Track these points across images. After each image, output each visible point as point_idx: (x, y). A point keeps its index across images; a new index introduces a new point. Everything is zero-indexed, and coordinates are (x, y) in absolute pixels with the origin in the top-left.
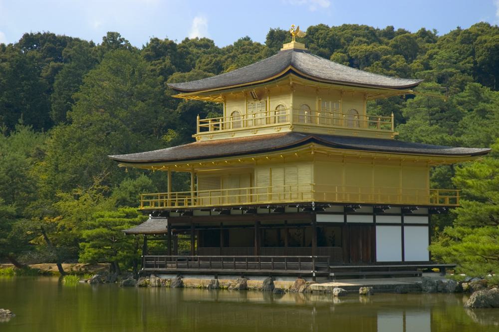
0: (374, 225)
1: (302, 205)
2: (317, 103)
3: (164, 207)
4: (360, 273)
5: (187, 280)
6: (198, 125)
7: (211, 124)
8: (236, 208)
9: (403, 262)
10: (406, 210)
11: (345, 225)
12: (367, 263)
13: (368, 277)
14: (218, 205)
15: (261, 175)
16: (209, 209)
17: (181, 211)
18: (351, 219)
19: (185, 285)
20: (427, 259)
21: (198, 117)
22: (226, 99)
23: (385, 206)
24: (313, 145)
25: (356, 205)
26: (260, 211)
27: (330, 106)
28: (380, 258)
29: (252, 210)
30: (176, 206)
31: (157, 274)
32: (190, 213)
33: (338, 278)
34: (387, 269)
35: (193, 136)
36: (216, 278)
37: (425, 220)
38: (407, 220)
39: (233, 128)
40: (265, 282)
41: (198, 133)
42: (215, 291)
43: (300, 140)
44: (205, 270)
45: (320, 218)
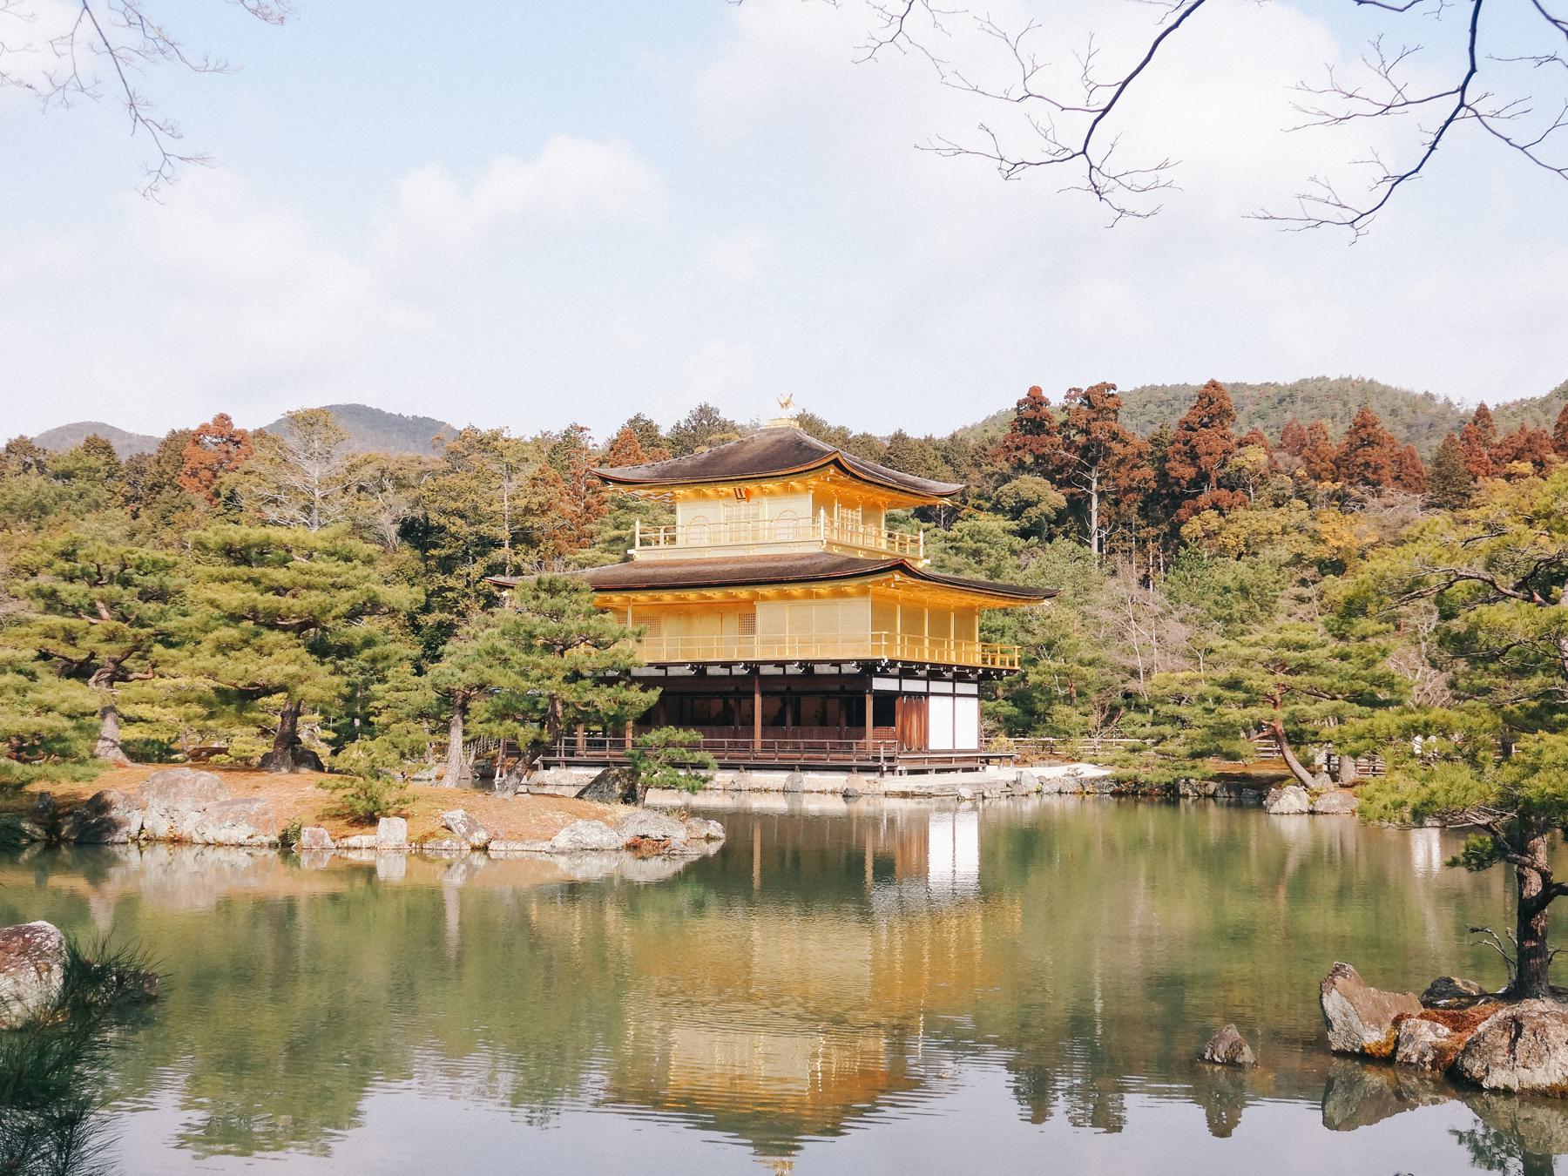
0: (927, 695)
1: (860, 663)
10: (961, 676)
11: (899, 694)
18: (910, 686)
20: (975, 747)
23: (949, 667)
24: (897, 577)
25: (922, 665)
26: (766, 670)
27: (848, 513)
29: (753, 667)
31: (569, 764)
33: (911, 772)
37: (973, 689)
38: (961, 688)
45: (879, 684)
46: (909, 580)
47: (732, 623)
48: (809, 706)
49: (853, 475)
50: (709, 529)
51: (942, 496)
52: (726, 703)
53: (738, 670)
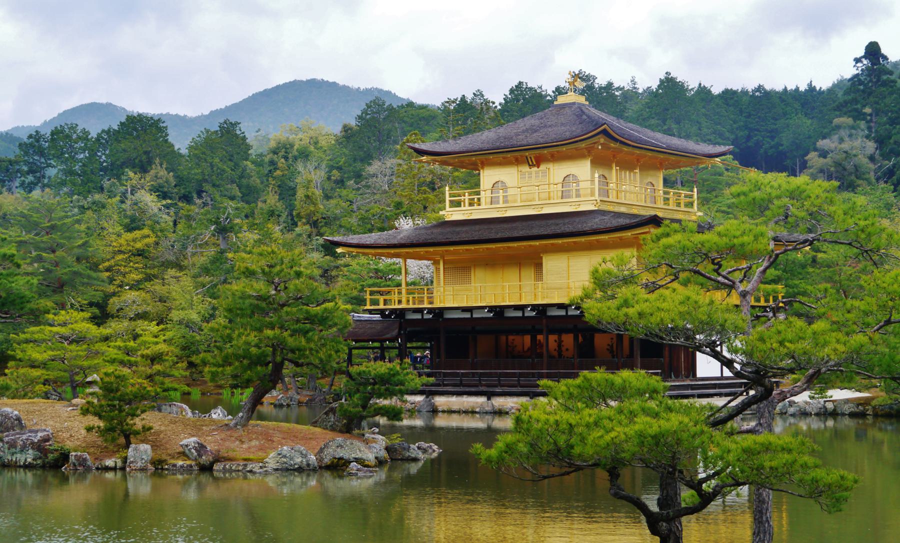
2: (614, 171)
3: (393, 307)
4: (690, 392)
5: (440, 401)
6: (448, 199)
7: (467, 197)
8: (521, 308)
9: (722, 378)
12: (687, 377)
13: (700, 396)
14: (493, 304)
15: (553, 264)
17: (430, 311)
19: (440, 409)
21: (447, 188)
22: (485, 164)
28: (700, 374)
29: (542, 309)
30: (426, 305)
32: (439, 313)
34: (714, 386)
35: (441, 213)
36: (489, 399)
39: (506, 201)
41: (448, 208)
42: (489, 417)
43: (628, 221)
44: (473, 389)
47: (528, 274)
48: (601, 341)
49: (622, 142)
52: (534, 339)
53: (529, 313)
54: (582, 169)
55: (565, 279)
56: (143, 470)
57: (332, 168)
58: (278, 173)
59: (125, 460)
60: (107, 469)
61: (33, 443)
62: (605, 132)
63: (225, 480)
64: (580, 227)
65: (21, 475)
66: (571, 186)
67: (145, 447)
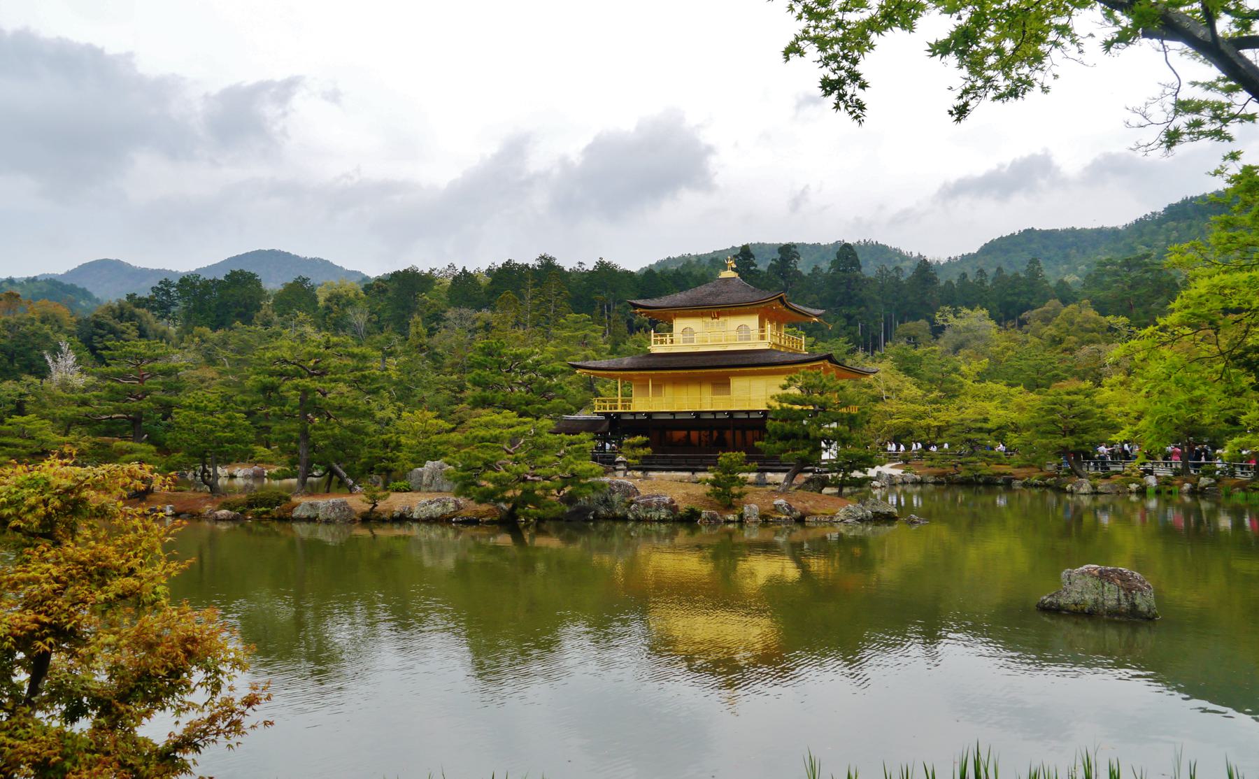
15: (737, 384)
16: (673, 413)
22: (676, 316)
40: (758, 477)
46: (829, 365)
50: (693, 335)
51: (816, 316)
54: (752, 322)
55: (752, 395)
56: (756, 522)
57: (372, 313)
58: (333, 315)
59: (741, 516)
60: (729, 522)
61: (665, 504)
62: (781, 299)
63: (810, 528)
64: (768, 360)
65: (656, 527)
66: (740, 333)
67: (754, 506)
